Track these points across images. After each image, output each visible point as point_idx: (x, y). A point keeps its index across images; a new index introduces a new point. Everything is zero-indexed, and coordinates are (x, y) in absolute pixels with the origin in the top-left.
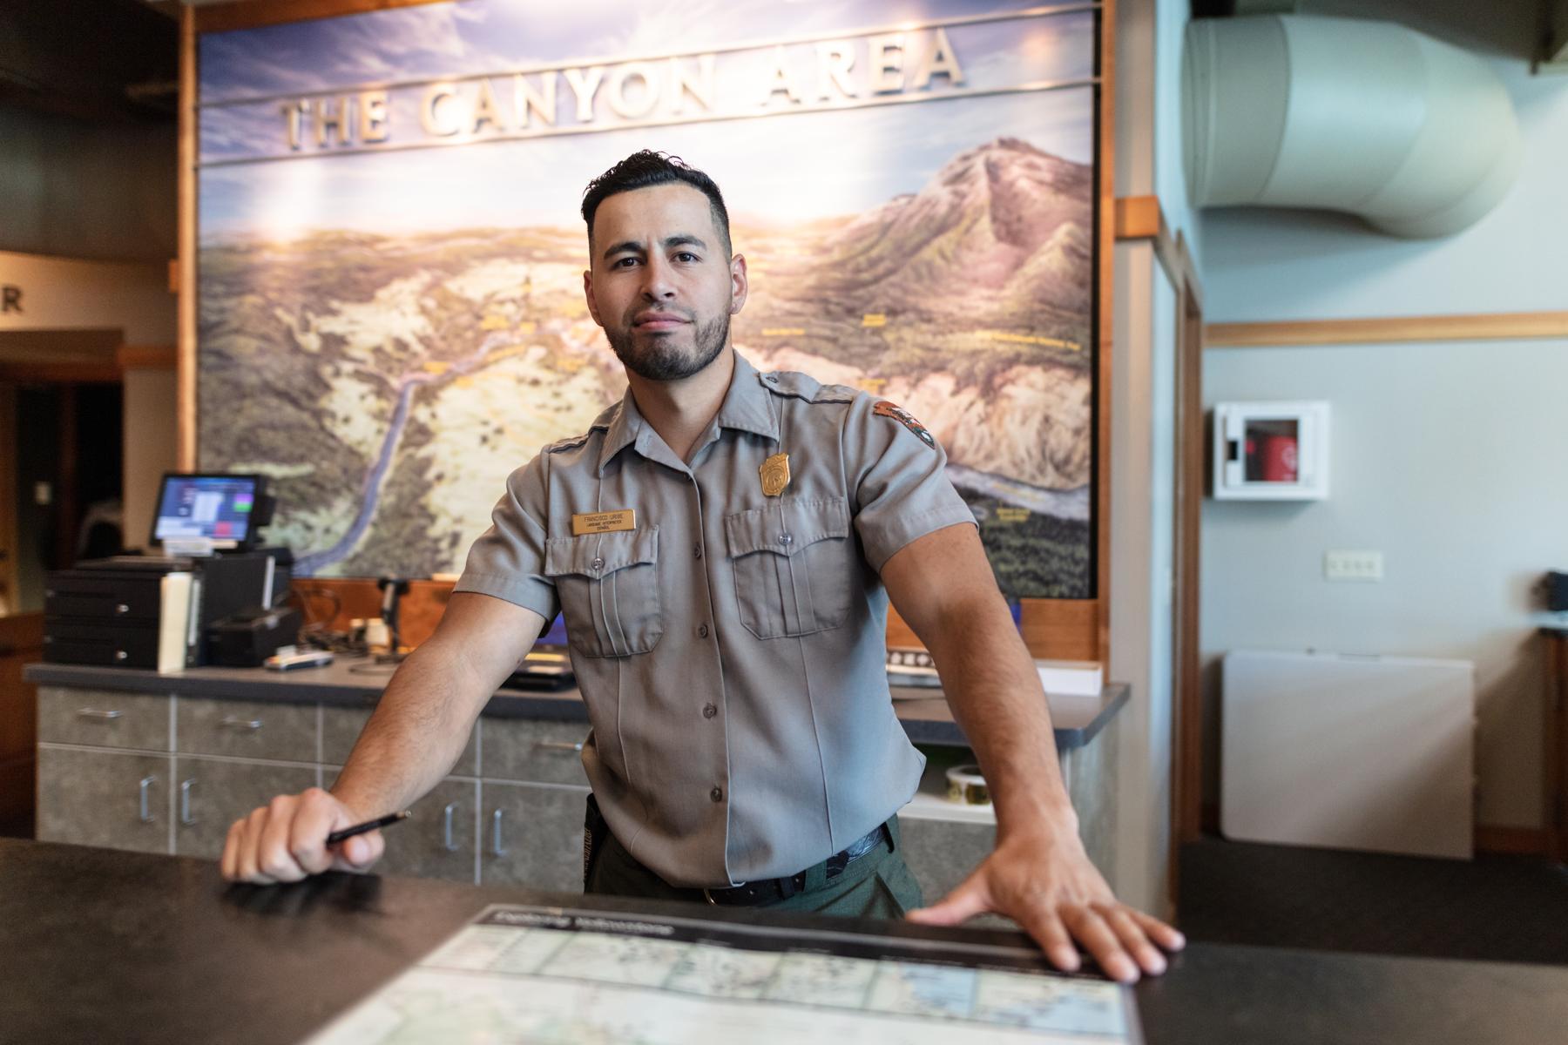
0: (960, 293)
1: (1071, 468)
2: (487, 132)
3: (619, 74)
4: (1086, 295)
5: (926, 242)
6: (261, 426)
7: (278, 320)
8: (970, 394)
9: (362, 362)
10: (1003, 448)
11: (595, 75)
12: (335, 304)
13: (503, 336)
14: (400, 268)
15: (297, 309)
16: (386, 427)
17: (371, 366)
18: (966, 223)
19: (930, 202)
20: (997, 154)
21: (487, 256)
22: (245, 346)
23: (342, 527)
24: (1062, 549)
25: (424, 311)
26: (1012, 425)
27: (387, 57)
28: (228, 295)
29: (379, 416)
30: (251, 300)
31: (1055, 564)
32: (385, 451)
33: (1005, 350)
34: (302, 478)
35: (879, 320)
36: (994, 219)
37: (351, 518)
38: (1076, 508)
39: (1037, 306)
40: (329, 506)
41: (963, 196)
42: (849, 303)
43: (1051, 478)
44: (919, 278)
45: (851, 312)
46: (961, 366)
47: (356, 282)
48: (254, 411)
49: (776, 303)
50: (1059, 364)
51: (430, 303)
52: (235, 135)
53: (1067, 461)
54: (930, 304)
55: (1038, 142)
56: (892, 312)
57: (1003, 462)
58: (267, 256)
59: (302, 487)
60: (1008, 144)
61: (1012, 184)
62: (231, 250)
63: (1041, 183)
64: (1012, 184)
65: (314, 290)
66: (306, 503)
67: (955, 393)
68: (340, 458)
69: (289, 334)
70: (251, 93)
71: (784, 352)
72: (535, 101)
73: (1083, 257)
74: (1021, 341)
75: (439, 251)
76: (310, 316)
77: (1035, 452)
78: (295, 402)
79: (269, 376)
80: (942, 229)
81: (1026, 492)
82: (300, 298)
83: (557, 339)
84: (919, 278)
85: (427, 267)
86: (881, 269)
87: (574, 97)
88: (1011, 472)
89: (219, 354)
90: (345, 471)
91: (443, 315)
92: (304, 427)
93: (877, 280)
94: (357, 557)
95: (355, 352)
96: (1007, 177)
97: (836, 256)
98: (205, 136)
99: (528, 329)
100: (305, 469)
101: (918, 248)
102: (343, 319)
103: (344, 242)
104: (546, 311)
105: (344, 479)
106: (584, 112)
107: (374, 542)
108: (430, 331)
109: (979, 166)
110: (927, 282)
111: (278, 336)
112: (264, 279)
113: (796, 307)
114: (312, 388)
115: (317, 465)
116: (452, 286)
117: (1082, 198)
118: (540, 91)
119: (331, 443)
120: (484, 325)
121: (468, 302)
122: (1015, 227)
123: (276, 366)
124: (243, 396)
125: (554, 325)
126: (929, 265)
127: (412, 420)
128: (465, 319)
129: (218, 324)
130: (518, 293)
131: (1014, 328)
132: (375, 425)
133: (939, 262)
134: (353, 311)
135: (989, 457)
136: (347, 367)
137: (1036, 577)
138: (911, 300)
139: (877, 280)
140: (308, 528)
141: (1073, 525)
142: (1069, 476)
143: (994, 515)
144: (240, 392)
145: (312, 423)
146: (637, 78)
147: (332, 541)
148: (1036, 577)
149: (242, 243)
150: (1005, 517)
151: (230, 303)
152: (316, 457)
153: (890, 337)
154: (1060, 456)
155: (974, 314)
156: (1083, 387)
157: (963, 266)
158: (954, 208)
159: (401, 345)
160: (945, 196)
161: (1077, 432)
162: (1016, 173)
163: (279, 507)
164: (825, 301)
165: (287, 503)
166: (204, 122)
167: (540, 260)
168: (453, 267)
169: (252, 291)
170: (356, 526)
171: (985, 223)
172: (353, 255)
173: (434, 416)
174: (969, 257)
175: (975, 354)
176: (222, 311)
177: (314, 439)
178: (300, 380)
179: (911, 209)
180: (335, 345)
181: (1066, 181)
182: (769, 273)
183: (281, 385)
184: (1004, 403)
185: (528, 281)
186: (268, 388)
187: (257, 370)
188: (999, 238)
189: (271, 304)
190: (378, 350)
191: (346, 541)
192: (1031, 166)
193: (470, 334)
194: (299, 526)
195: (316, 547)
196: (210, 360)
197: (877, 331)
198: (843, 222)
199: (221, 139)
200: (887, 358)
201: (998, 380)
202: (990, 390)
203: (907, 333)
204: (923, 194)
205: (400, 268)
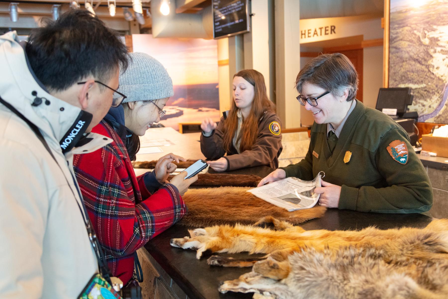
6: (409, 71)
7: (415, 35)
12: (435, 27)
15: (422, 29)
22: (404, 44)
23: (435, 106)
28: (399, 28)
30: (406, 28)
34: (422, 88)
37: (438, 102)
40: (431, 98)
47: (443, 18)
48: (406, 66)
58: (412, 12)
59: (422, 92)
62: (400, 12)
65: (427, 22)
66: (423, 97)
68: (435, 82)
69: (419, 39)
76: (426, 32)
78: (420, 62)
79: (412, 54)
89: (396, 48)
90: (437, 86)
92: (423, 71)
94: (440, 116)
95: (440, 43)
100: (423, 85)
102: (437, 32)
105: (436, 89)
111: (415, 40)
112: (411, 21)
114: (426, 57)
115: (427, 84)
119: (432, 76)
124: (404, 61)
129: (396, 38)
136: (438, 49)
140: (424, 106)
144: (402, 60)
145: (427, 70)
147: (431, 110)
149: (404, 9)
151: (400, 30)
152: (427, 81)
163: (414, 99)
165: (417, 97)
169: (407, 26)
170: (440, 105)
176: (397, 33)
177: (426, 75)
178: (422, 55)
180: (434, 41)
183: (415, 57)
186: (411, 58)
187: (408, 53)
189: (413, 29)
191: (436, 110)
194: (420, 105)
195: (426, 112)
196: (393, 50)
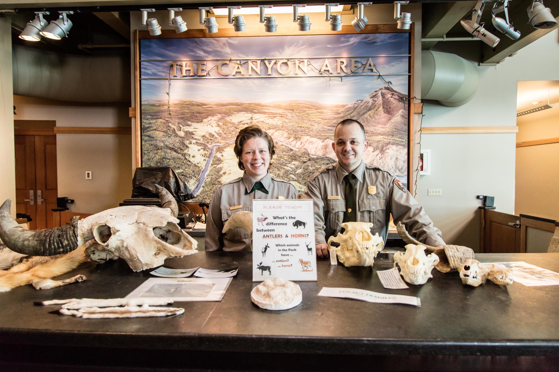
0: (375, 126)
1: (403, 171)
4: (407, 127)
5: (366, 113)
8: (377, 152)
9: (199, 140)
10: (386, 166)
12: (189, 123)
15: (176, 123)
16: (207, 159)
17: (202, 141)
18: (376, 108)
20: (384, 91)
21: (239, 111)
25: (218, 126)
26: (388, 159)
27: (205, 52)
28: (152, 119)
29: (204, 155)
32: (207, 165)
33: (387, 141)
36: (383, 108)
37: (196, 185)
39: (394, 130)
41: (376, 101)
46: (375, 145)
49: (325, 127)
51: (221, 124)
52: (154, 71)
53: (402, 169)
61: (388, 99)
63: (395, 99)
64: (388, 99)
65: (182, 118)
67: (373, 152)
68: (191, 168)
71: (327, 140)
73: (406, 118)
74: (390, 139)
75: (224, 109)
77: (394, 167)
80: (370, 110)
82: (177, 121)
85: (219, 113)
87: (267, 68)
89: (149, 136)
91: (226, 127)
97: (342, 115)
98: (142, 70)
101: (364, 114)
102: (192, 127)
103: (193, 105)
106: (269, 72)
107: (203, 192)
108: (221, 131)
109: (380, 94)
110: (366, 123)
113: (331, 128)
119: (188, 163)
121: (233, 124)
122: (389, 110)
123: (170, 141)
126: (367, 118)
127: (215, 157)
129: (148, 128)
132: (203, 158)
133: (369, 117)
134: (195, 125)
142: (402, 173)
144: (157, 148)
152: (184, 167)
154: (400, 167)
155: (378, 131)
156: (406, 150)
157: (375, 119)
158: (373, 104)
160: (371, 101)
161: (404, 162)
166: (142, 66)
167: (255, 113)
168: (229, 113)
171: (381, 107)
173: (222, 156)
174: (377, 117)
175: (378, 141)
178: (177, 145)
180: (190, 134)
181: (401, 98)
182: (322, 119)
184: (386, 154)
185: (252, 118)
186: (167, 147)
188: (385, 112)
190: (203, 136)
193: (233, 133)
198: (343, 106)
199: (149, 72)
201: (384, 148)
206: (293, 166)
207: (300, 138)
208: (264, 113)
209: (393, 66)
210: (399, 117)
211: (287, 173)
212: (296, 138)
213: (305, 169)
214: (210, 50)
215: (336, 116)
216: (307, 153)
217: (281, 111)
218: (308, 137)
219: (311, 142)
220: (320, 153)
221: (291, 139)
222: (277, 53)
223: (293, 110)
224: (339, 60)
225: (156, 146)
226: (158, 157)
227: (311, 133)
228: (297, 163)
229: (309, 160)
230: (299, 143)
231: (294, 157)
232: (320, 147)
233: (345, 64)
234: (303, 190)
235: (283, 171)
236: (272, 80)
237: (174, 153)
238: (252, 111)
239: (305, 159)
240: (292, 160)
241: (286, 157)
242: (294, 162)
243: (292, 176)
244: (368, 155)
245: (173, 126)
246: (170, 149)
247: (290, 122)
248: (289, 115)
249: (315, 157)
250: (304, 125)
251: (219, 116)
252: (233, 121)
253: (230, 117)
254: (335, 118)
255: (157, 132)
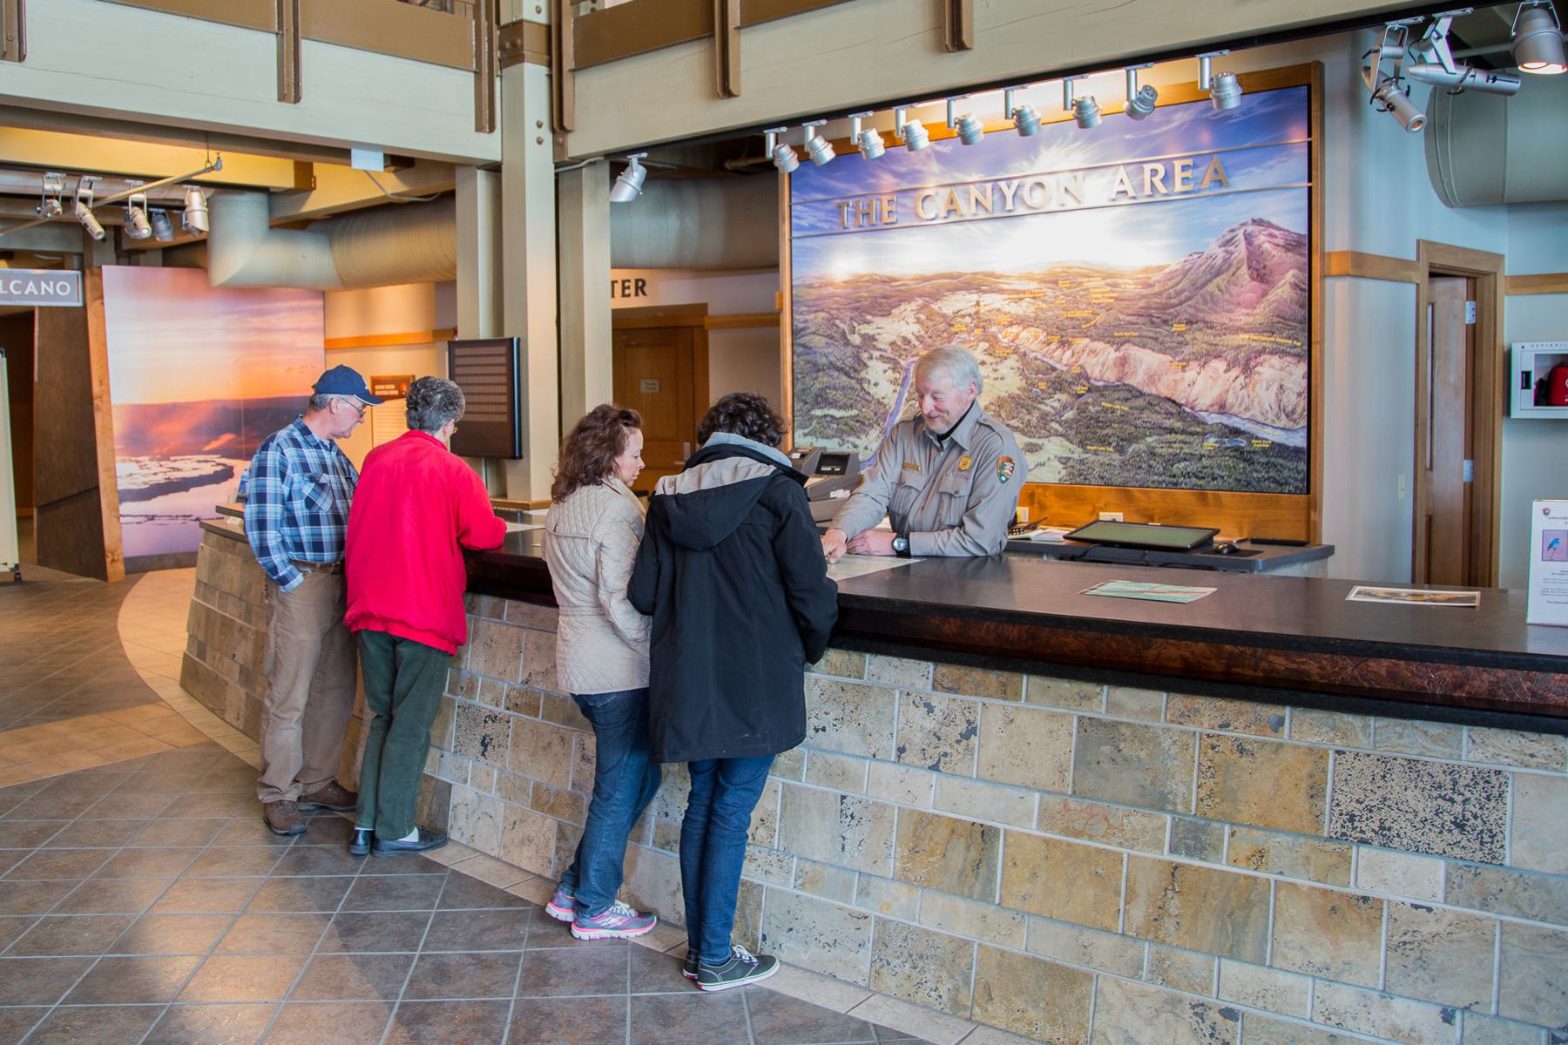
0: (1230, 311)
2: (953, 218)
3: (1029, 182)
4: (1305, 312)
5: (1210, 281)
8: (1235, 372)
11: (1015, 183)
12: (869, 317)
13: (964, 336)
14: (904, 296)
17: (889, 354)
18: (1233, 269)
19: (1212, 257)
20: (1250, 228)
21: (955, 289)
24: (1289, 464)
25: (919, 321)
26: (1260, 389)
28: (809, 312)
31: (1286, 473)
32: (898, 403)
33: (1258, 346)
34: (852, 418)
35: (1182, 327)
38: (1299, 440)
42: (1164, 317)
43: (1284, 422)
44: (1205, 302)
45: (1165, 322)
46: (1231, 355)
48: (824, 379)
50: (1290, 354)
51: (923, 317)
52: (812, 220)
53: (1293, 412)
54: (1212, 318)
55: (1274, 221)
56: (1189, 322)
57: (1255, 412)
60: (1258, 222)
65: (857, 309)
67: (1226, 371)
70: (820, 196)
72: (981, 198)
74: (1266, 340)
75: (927, 286)
78: (847, 374)
80: (1218, 274)
81: (1269, 430)
83: (996, 338)
84: (1205, 302)
85: (920, 296)
86: (1183, 296)
87: (1004, 197)
88: (1261, 419)
89: (804, 346)
93: (1181, 303)
96: (1257, 242)
97: (1156, 289)
99: (978, 332)
100: (854, 412)
104: (989, 321)
106: (1009, 206)
109: (1241, 236)
113: (1133, 319)
116: (935, 307)
117: (1302, 255)
118: (984, 194)
120: (953, 330)
121: (944, 316)
123: (837, 354)
125: (994, 329)
128: (942, 326)
130: (972, 311)
131: (1262, 332)
132: (892, 387)
134: (878, 321)
135: (1247, 409)
136: (876, 354)
137: (1276, 481)
138: (1201, 315)
139: (1181, 303)
141: (1297, 450)
143: (1250, 444)
144: (817, 368)
146: (1040, 185)
148: (1276, 481)
150: (1257, 445)
153: (1188, 337)
154: (1289, 409)
156: (1303, 367)
158: (1225, 260)
159: (906, 341)
160: (1220, 253)
161: (1299, 395)
162: (1262, 239)
164: (1150, 316)
167: (985, 292)
168: (936, 296)
171: (1244, 268)
172: (879, 289)
175: (1238, 347)
179: (1200, 261)
180: (869, 340)
181: (1291, 245)
182: (1117, 299)
185: (978, 304)
186: (832, 366)
189: (833, 318)
190: (893, 344)
192: (1271, 235)
196: (799, 350)
197: (1180, 334)
198: (1160, 269)
199: (804, 223)
200: (1187, 350)
201: (1252, 364)
202: (1247, 369)
203: (1198, 335)
204: (1207, 252)
205: (904, 296)
206: (1056, 404)
207: (1070, 344)
208: (1001, 291)
209: (1271, 167)
210: (1287, 288)
211: (1044, 417)
212: (1064, 344)
213: (1082, 411)
214: (903, 170)
215: (1145, 292)
216: (1083, 376)
217: (1033, 286)
218: (1087, 341)
219: (1093, 352)
220: (1111, 376)
221: (1053, 346)
222: (1025, 163)
223: (1056, 282)
224: (1147, 167)
225: (815, 364)
226: (818, 385)
227: (1093, 332)
228: (1064, 397)
229: (1089, 390)
230: (1069, 353)
231: (1059, 385)
232: (1110, 363)
233: (1161, 174)
234: (1076, 456)
235: (1036, 414)
236: (1016, 221)
237: (844, 378)
238: (979, 290)
239: (1080, 390)
240: (1056, 390)
241: (1043, 385)
242: (1058, 396)
243: (1055, 426)
244: (1215, 380)
245: (842, 326)
246: (839, 369)
247: (1050, 309)
248: (1050, 293)
249: (1101, 384)
250: (1079, 314)
251: (920, 302)
252: (945, 311)
253: (939, 304)
254: (1143, 297)
255: (817, 338)
